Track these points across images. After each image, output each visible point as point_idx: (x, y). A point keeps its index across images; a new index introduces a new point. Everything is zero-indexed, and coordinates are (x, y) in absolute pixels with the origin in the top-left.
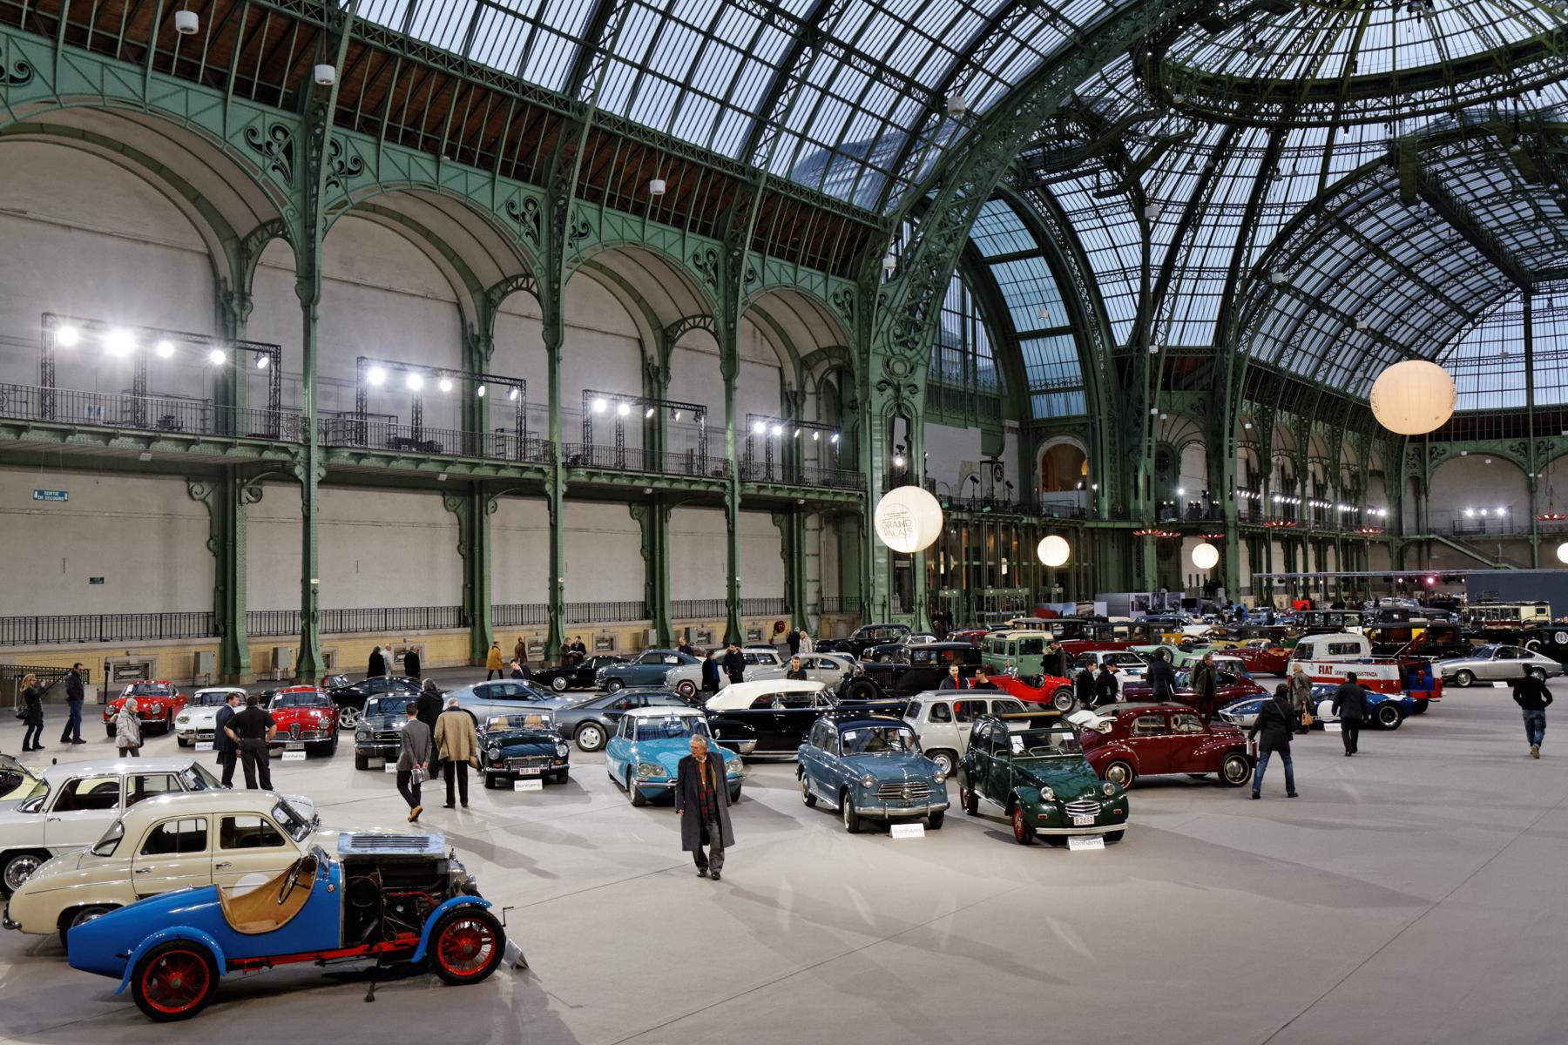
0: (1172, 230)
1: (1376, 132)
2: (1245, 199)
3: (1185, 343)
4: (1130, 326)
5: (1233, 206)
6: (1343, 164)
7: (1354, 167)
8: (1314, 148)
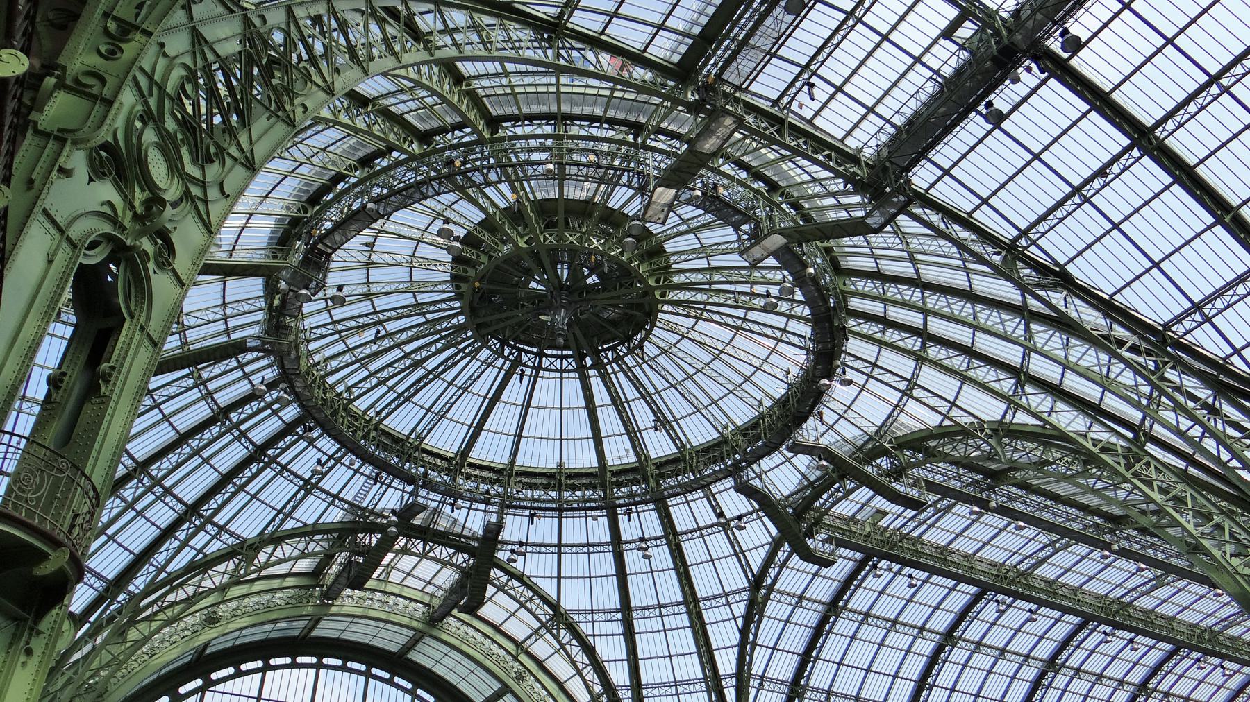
2: (190, 498)
6: (311, 511)
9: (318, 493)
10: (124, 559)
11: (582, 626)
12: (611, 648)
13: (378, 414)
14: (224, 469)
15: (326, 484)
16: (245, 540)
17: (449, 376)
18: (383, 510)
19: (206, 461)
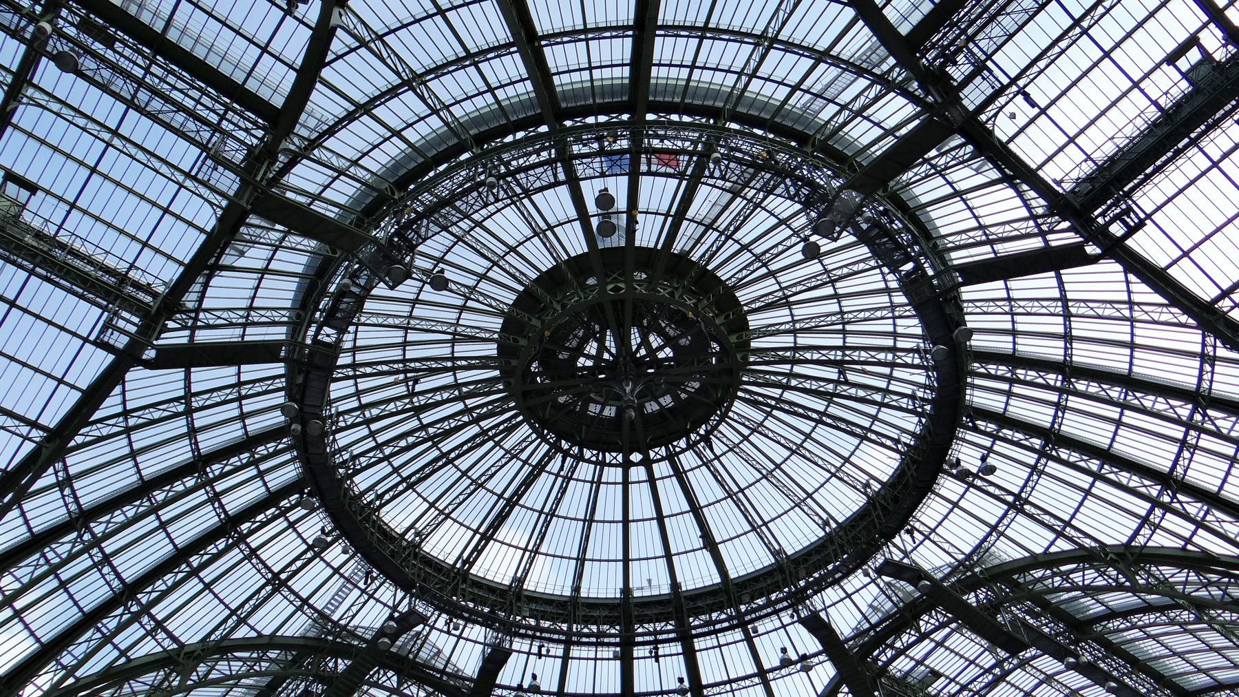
6: (273, 617)
7: (267, 632)
9: (286, 592)
13: (380, 497)
15: (296, 584)
17: (464, 463)
18: (357, 627)
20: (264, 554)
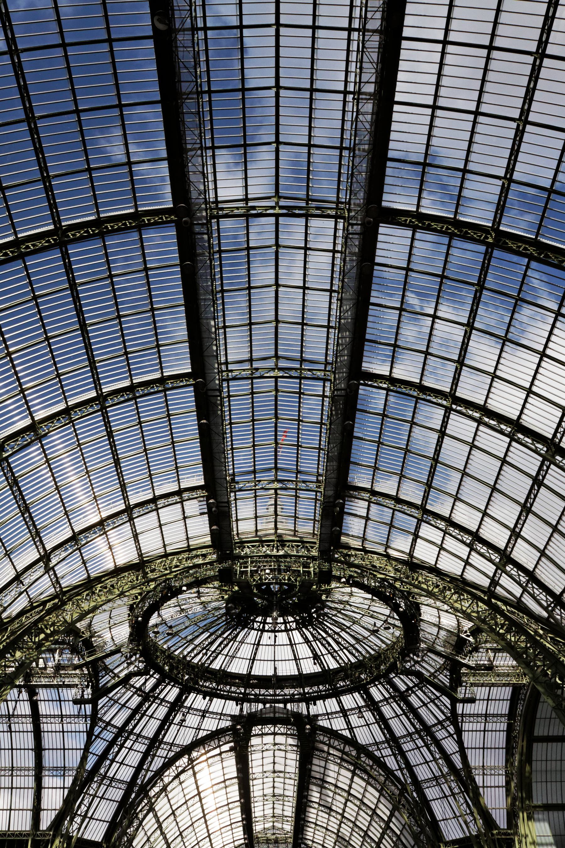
0: (104, 745)
1: (232, 708)
2: (151, 735)
3: (85, 837)
4: (54, 814)
5: (144, 737)
6: (210, 724)
7: (214, 729)
8: (197, 710)
10: (131, 771)
11: (376, 753)
12: (391, 763)
14: (161, 717)
16: (186, 746)
19: (151, 717)
20: (195, 706)
